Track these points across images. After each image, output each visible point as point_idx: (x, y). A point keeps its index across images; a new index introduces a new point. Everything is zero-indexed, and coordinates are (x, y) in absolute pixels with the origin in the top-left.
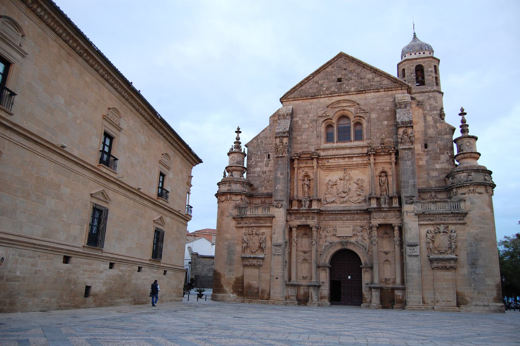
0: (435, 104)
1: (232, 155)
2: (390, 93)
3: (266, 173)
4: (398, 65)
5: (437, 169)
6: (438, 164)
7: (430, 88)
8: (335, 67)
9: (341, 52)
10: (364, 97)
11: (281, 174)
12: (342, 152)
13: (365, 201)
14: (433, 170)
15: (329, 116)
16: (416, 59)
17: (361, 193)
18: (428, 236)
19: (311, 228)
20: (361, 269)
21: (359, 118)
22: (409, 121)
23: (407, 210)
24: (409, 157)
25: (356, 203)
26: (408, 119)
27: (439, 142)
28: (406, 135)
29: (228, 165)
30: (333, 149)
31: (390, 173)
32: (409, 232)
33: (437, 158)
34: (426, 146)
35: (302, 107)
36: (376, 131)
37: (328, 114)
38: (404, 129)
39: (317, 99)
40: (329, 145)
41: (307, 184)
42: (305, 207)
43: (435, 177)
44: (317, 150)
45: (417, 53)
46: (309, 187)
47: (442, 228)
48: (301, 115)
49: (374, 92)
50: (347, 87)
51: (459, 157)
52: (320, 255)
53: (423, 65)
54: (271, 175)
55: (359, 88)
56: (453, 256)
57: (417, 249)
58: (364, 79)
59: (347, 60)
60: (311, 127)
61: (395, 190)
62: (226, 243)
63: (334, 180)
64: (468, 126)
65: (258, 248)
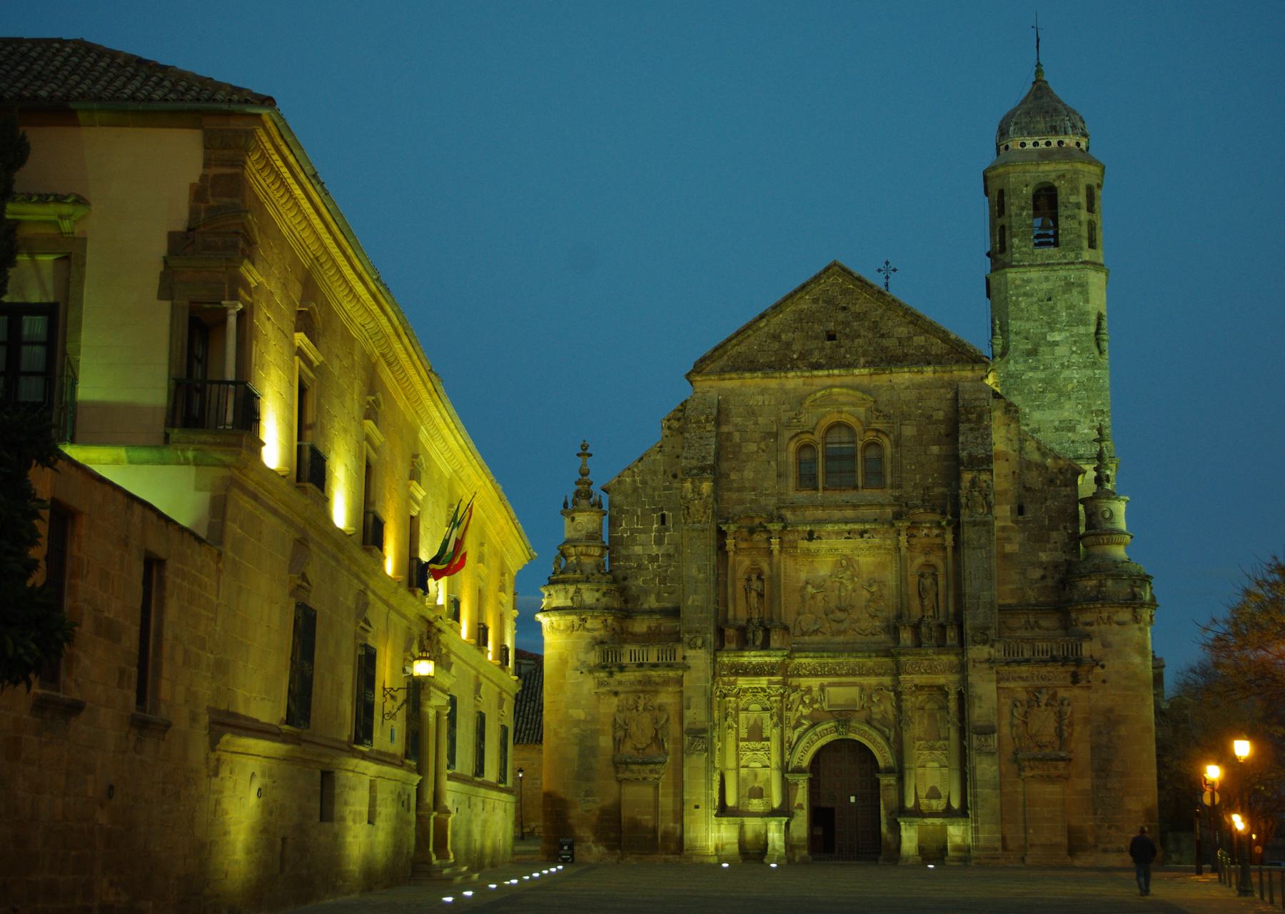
0: (1081, 304)
3: (658, 561)
5: (1042, 563)
8: (821, 302)
9: (835, 261)
10: (889, 383)
11: (699, 571)
17: (878, 614)
18: (1015, 713)
20: (879, 780)
21: (875, 434)
23: (974, 656)
24: (983, 540)
25: (866, 635)
27: (1048, 503)
28: (977, 489)
31: (941, 570)
32: (977, 704)
35: (741, 397)
36: (913, 467)
38: (975, 473)
39: (778, 381)
40: (804, 495)
41: (756, 591)
42: (754, 643)
44: (779, 508)
47: (1044, 698)
48: (739, 420)
49: (909, 372)
50: (848, 356)
53: (1056, 184)
54: (670, 565)
55: (877, 360)
56: (1063, 754)
57: (993, 741)
58: (889, 337)
59: (850, 284)
60: (763, 451)
62: (576, 730)
65: (649, 742)
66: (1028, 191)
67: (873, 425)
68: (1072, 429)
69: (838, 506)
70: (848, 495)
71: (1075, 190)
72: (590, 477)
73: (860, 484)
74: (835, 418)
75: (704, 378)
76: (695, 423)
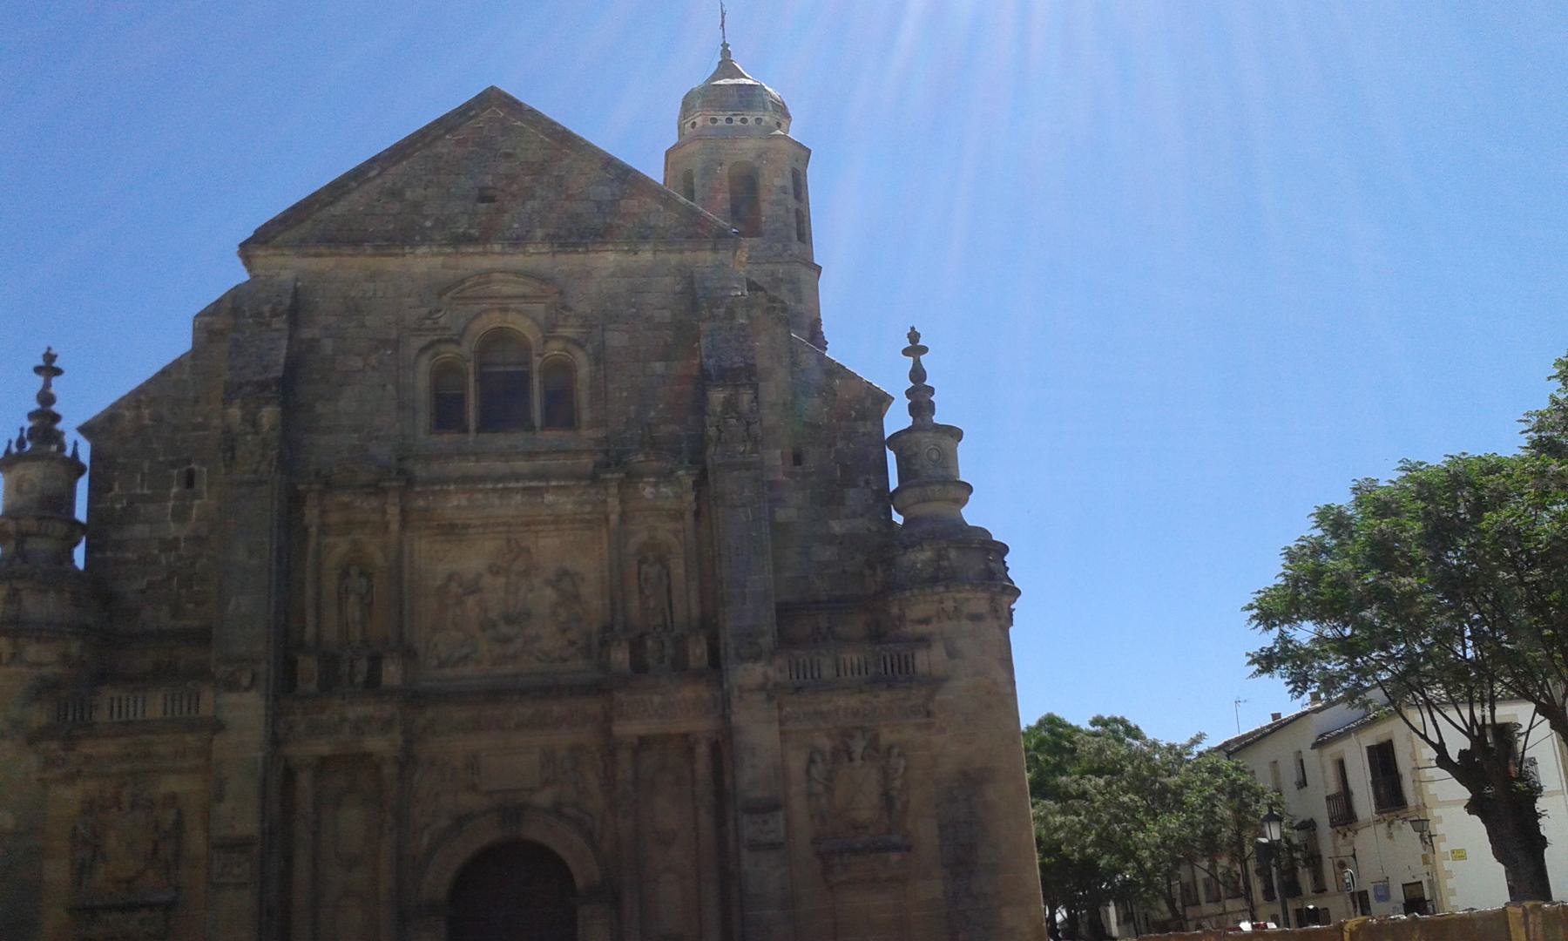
2: (674, 259)
4: (668, 153)
6: (839, 518)
7: (780, 246)
8: (470, 143)
12: (499, 467)
15: (449, 329)
22: (742, 365)
26: (741, 359)
27: (840, 445)
28: (734, 414)
34: (798, 459)
36: (625, 394)
37: (442, 321)
39: (399, 261)
40: (447, 439)
45: (734, 118)
49: (617, 251)
51: (910, 495)
56: (896, 839)
60: (373, 368)
64: (933, 394)
67: (559, 330)
70: (518, 439)
72: (56, 408)
74: (493, 320)
75: (271, 251)
76: (251, 316)
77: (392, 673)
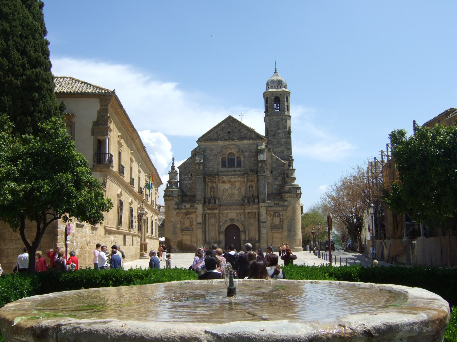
1: (171, 175)
2: (255, 142)
4: (264, 93)
12: (231, 173)
13: (242, 200)
14: (274, 185)
16: (275, 92)
19: (216, 214)
27: (278, 170)
29: (168, 180)
30: (226, 171)
31: (254, 185)
33: (276, 179)
43: (275, 188)
46: (214, 192)
47: (277, 215)
52: (220, 227)
53: (280, 96)
56: (281, 227)
57: (265, 224)
61: (256, 195)
63: (226, 188)
66: (273, 98)
68: (283, 153)
69: (231, 171)
70: (233, 169)
71: (284, 98)
72: (174, 165)
73: (236, 166)
74: (230, 151)
77: (217, 202)
